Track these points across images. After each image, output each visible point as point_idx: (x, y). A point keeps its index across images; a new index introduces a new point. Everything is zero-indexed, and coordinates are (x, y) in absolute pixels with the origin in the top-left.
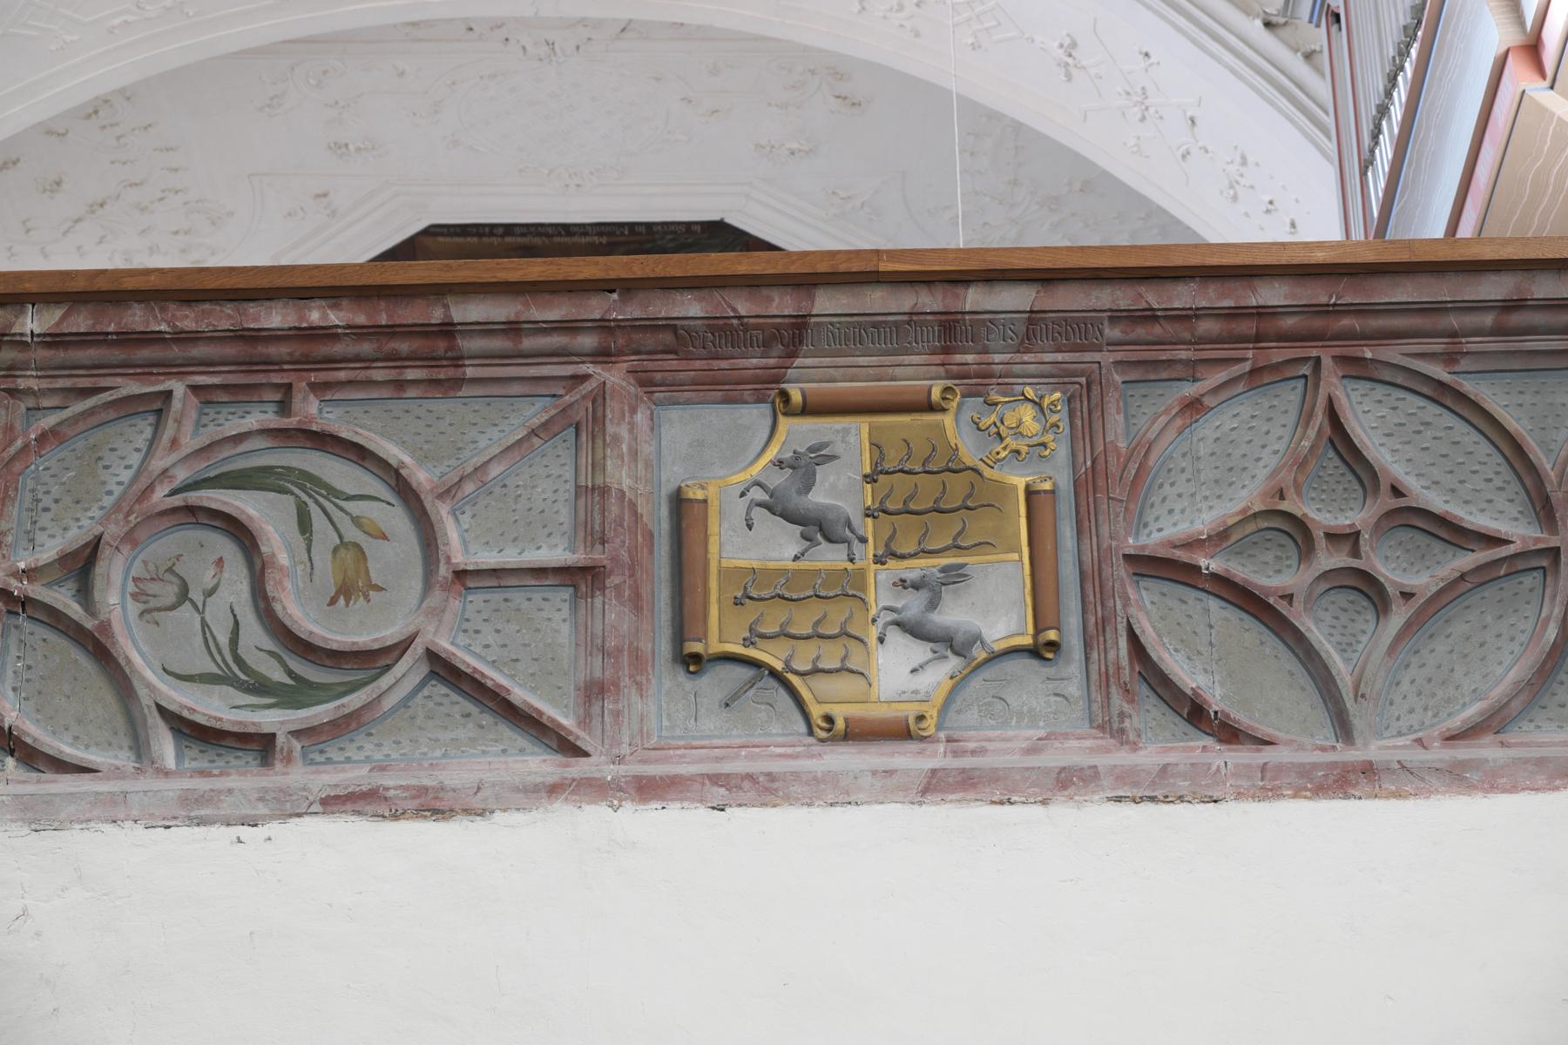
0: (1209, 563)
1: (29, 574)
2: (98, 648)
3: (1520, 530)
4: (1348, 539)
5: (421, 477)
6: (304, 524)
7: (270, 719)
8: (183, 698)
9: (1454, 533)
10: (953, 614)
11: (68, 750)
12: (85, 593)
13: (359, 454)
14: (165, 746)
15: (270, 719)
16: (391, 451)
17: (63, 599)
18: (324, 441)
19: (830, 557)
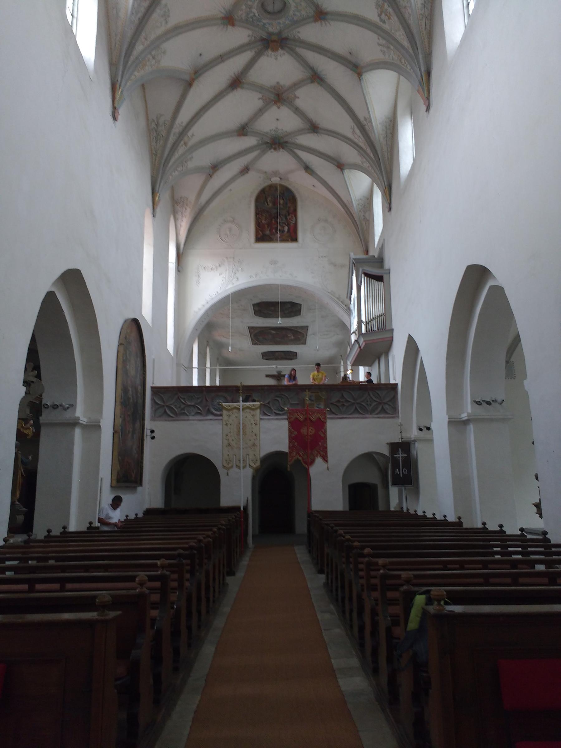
0: (335, 403)
1: (266, 403)
2: (270, 408)
3: (353, 401)
4: (342, 402)
5: (288, 397)
6: (281, 399)
7: (281, 413)
8: (275, 411)
9: (349, 402)
10: (320, 406)
11: (270, 415)
12: (269, 405)
13: (285, 396)
14: (274, 414)
15: (281, 413)
16: (286, 395)
17: (268, 405)
18: (283, 395)
19: (313, 402)
